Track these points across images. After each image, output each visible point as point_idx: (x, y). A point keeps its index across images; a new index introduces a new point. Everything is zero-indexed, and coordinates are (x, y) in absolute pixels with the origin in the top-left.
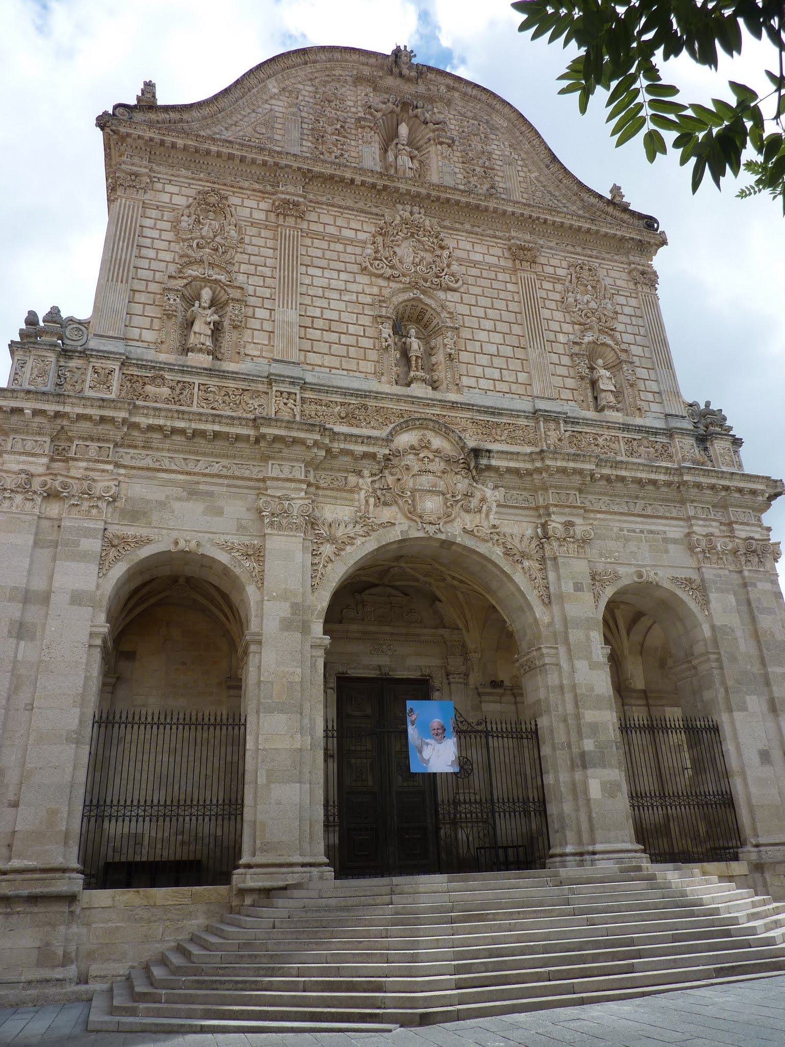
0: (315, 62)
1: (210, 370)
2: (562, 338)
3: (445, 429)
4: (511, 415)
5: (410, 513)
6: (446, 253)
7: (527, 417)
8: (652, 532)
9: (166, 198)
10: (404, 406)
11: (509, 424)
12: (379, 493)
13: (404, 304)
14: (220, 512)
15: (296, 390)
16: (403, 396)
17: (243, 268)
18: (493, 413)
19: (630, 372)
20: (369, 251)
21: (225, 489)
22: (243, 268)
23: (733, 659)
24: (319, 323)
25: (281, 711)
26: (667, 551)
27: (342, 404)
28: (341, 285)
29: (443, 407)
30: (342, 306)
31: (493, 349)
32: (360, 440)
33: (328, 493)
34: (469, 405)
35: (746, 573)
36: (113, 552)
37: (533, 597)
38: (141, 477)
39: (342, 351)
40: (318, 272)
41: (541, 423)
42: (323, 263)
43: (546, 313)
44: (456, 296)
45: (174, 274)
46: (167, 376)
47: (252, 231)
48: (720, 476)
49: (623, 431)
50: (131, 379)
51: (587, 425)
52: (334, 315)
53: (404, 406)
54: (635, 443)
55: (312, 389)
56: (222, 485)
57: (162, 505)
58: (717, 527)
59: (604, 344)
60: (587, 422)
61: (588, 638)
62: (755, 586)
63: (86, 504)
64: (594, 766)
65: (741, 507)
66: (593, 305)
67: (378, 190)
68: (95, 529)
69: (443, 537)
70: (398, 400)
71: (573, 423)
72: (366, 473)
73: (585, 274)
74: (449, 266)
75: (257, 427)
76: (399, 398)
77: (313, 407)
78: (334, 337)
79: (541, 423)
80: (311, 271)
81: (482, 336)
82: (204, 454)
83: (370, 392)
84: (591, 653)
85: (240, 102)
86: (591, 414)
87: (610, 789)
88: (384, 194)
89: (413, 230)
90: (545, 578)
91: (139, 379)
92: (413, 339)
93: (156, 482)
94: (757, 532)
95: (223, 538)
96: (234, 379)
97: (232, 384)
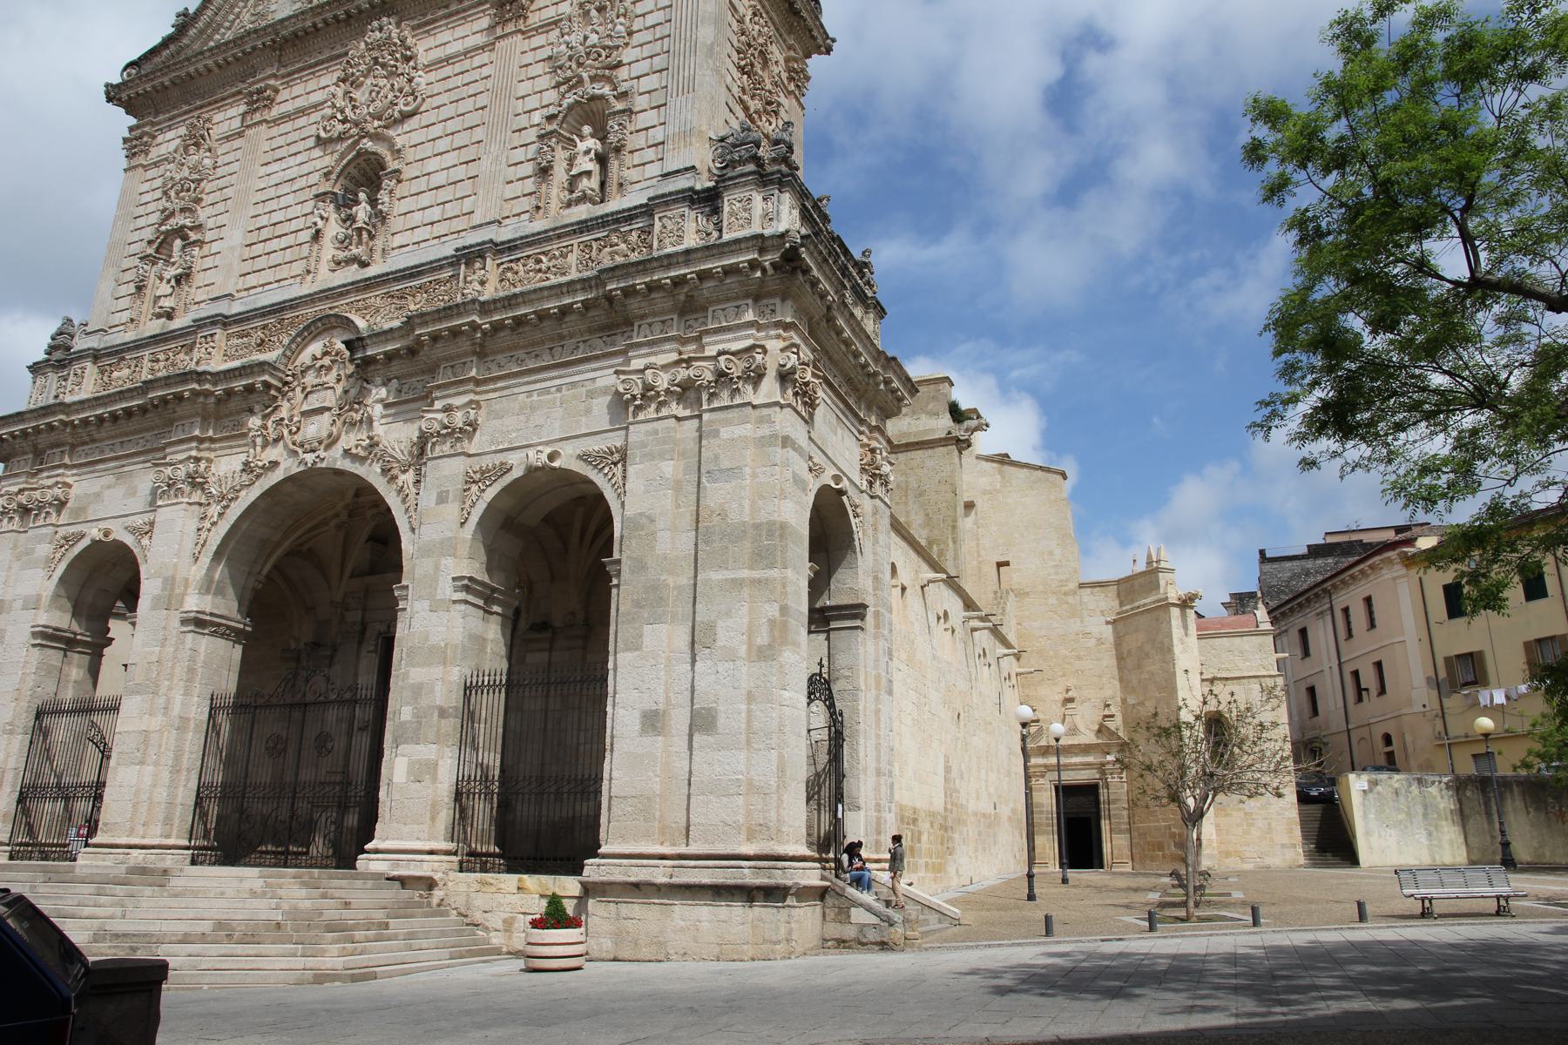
1: (154, 336)
4: (433, 270)
5: (294, 444)
7: (451, 264)
13: (353, 165)
16: (316, 293)
19: (616, 127)
21: (141, 466)
23: (640, 566)
24: (265, 234)
25: (138, 693)
26: (588, 411)
27: (264, 327)
29: (358, 290)
32: (237, 373)
34: (383, 275)
41: (463, 266)
44: (413, 122)
45: (151, 238)
48: (665, 263)
49: (582, 232)
51: (530, 244)
54: (595, 245)
55: (236, 322)
57: (98, 495)
58: (671, 351)
59: (593, 98)
61: (437, 568)
62: (716, 433)
64: (405, 742)
65: (728, 300)
67: (344, 21)
68: (46, 534)
70: (313, 301)
71: (509, 248)
72: (257, 408)
79: (463, 266)
82: (132, 433)
83: (284, 302)
87: (431, 769)
88: (352, 21)
91: (108, 368)
92: (364, 204)
94: (747, 337)
96: (174, 338)
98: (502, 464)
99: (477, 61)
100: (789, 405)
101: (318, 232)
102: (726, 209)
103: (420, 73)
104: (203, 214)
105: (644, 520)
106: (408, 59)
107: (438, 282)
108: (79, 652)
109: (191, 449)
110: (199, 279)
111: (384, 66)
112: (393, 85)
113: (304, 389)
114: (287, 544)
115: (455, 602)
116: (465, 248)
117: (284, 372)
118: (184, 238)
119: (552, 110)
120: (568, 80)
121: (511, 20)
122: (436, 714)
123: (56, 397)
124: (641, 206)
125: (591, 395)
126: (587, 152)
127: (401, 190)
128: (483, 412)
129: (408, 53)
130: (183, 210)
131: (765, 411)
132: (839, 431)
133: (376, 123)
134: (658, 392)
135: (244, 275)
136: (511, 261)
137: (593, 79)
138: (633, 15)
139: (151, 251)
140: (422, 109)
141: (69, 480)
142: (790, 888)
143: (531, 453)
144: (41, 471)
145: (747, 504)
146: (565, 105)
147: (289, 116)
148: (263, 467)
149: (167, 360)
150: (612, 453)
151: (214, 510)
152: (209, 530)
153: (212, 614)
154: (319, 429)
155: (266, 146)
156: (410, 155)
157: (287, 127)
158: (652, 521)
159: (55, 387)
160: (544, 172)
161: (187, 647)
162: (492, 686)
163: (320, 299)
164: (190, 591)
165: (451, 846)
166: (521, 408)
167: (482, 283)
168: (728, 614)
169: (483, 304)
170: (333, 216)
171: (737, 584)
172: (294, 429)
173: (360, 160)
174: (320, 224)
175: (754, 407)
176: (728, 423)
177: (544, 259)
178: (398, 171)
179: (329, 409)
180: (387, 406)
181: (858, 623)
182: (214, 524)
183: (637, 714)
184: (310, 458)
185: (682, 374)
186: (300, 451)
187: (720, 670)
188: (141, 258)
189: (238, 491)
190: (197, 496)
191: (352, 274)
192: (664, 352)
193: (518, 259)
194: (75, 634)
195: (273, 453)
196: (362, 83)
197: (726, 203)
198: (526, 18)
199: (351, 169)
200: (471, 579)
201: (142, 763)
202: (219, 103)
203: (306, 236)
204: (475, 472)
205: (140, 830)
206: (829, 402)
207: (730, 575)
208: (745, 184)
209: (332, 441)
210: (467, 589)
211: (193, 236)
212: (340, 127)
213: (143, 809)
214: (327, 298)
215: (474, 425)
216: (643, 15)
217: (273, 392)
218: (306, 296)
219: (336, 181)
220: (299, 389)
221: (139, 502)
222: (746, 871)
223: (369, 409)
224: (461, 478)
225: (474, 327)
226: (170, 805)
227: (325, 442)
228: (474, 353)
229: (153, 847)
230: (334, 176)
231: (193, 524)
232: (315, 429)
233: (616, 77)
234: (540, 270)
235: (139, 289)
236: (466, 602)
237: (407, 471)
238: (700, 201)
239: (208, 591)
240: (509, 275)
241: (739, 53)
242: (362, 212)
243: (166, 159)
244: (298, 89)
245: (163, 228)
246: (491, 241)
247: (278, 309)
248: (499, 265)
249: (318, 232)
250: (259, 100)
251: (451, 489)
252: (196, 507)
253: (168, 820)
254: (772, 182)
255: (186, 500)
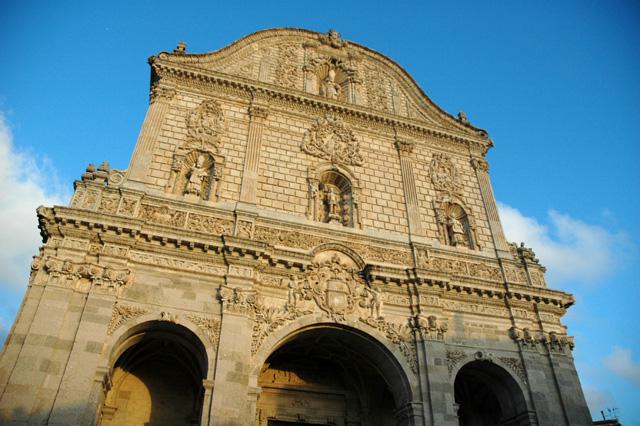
2: (429, 199)
3: (349, 253)
6: (356, 143)
7: (405, 247)
8: (488, 326)
9: (183, 104)
10: (323, 235)
12: (303, 291)
14: (193, 297)
15: (252, 220)
17: (226, 145)
20: (307, 139)
21: (198, 281)
22: (226, 145)
24: (271, 181)
27: (283, 232)
28: (287, 159)
30: (287, 171)
31: (384, 203)
33: (269, 289)
35: (552, 357)
36: (120, 318)
37: (407, 368)
38: (145, 270)
39: (285, 198)
40: (273, 150)
42: (277, 145)
43: (418, 183)
44: (360, 169)
46: (170, 207)
47: (233, 124)
50: (147, 207)
52: (282, 177)
53: (323, 235)
56: (197, 279)
60: (444, 252)
62: (558, 365)
63: (106, 284)
66: (448, 179)
69: (345, 323)
73: (443, 161)
74: (357, 151)
75: (223, 242)
76: (321, 230)
77: (263, 232)
78: (280, 189)
80: (268, 149)
81: (378, 194)
86: (448, 247)
89: (336, 129)
90: (417, 355)
95: (194, 314)
96: (213, 212)
97: (211, 215)
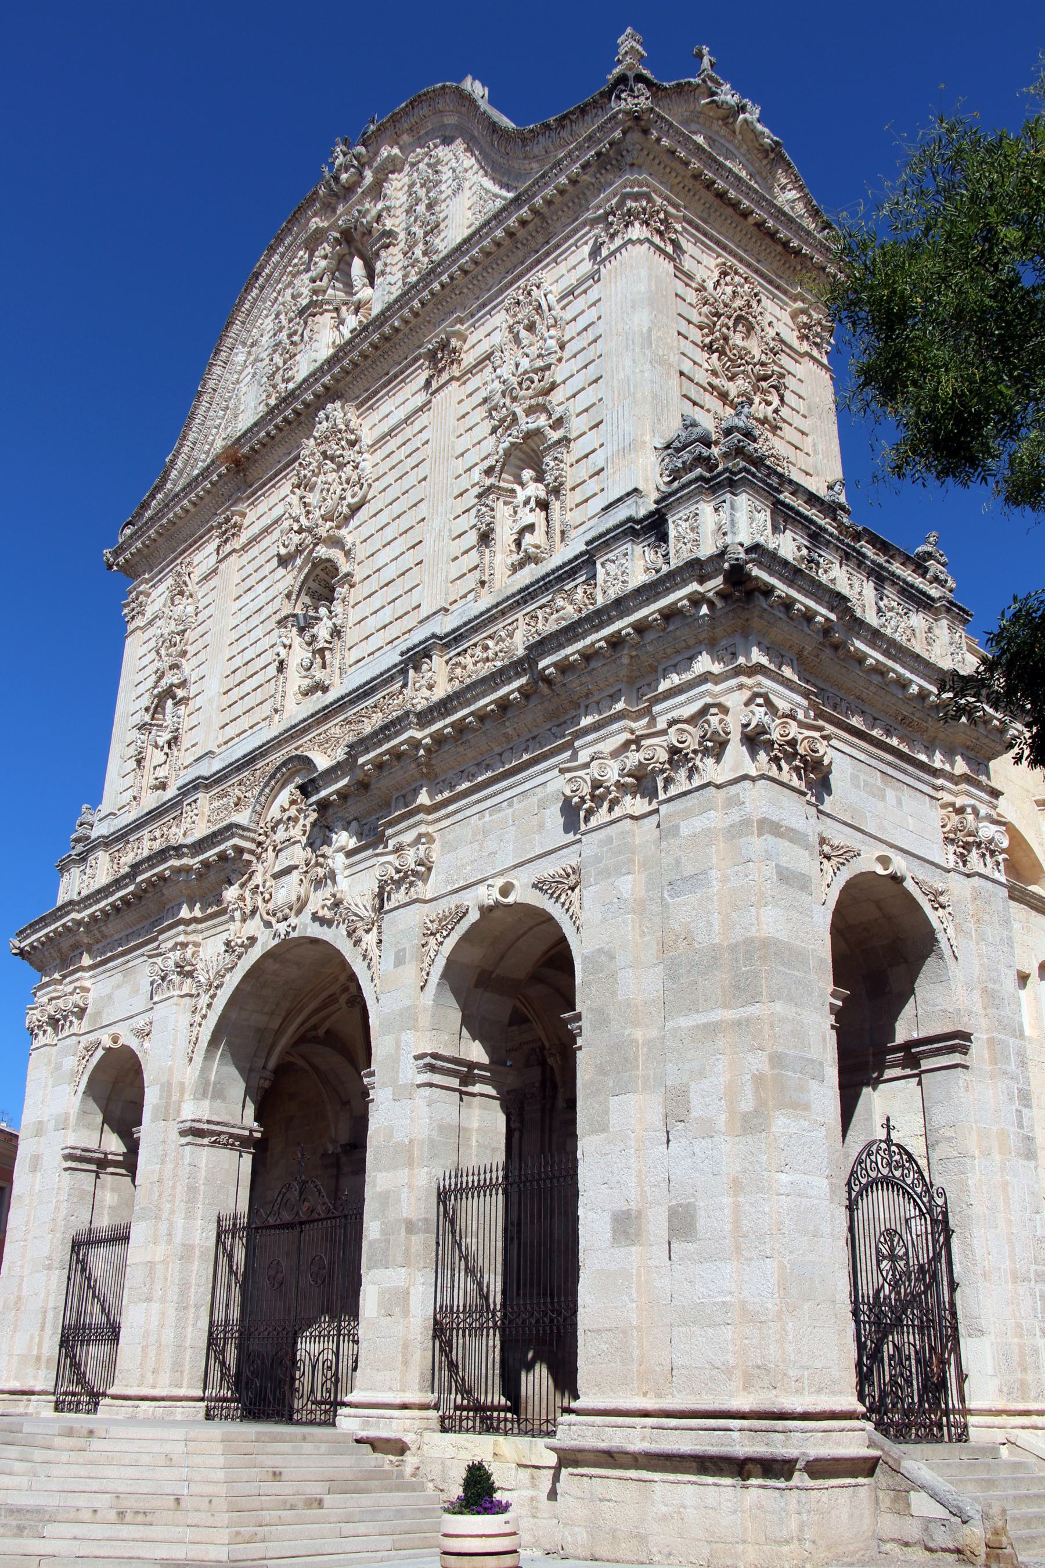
0: (269, 276)
5: (268, 914)
11: (384, 697)
16: (281, 734)
18: (366, 694)
19: (552, 464)
23: (603, 1020)
24: (239, 676)
26: (541, 826)
49: (526, 602)
51: (475, 630)
57: (110, 997)
59: (529, 435)
61: (398, 1046)
62: (675, 831)
71: (455, 639)
84: (397, 1072)
85: (211, 413)
93: (108, 974)
96: (167, 811)
98: (457, 907)
99: (417, 426)
100: (762, 777)
101: (281, 662)
102: (672, 533)
103: (366, 456)
104: (187, 666)
105: (603, 957)
106: (352, 444)
107: (391, 695)
108: (112, 1174)
109: (178, 934)
110: (186, 741)
111: (332, 459)
112: (340, 477)
113: (275, 847)
114: (291, 1030)
115: (419, 1086)
116: (409, 650)
117: (255, 832)
118: (174, 697)
119: (491, 461)
120: (502, 421)
121: (444, 368)
122: (403, 1230)
123: (79, 893)
124: (582, 554)
125: (543, 805)
126: (527, 502)
127: (354, 595)
128: (436, 847)
129: (353, 437)
130: (171, 668)
131: (734, 789)
132: (890, 794)
133: (329, 524)
134: (607, 788)
135: (223, 727)
136: (459, 654)
137: (530, 411)
138: (563, 323)
139: (147, 718)
140: (369, 497)
141: (87, 984)
142: (796, 1460)
143: (482, 889)
144: (64, 977)
145: (716, 919)
146: (501, 452)
147: (255, 539)
148: (242, 946)
149: (162, 836)
150: (568, 875)
151: (204, 1000)
152: (200, 1025)
153: (209, 1122)
154: (288, 893)
155: (237, 578)
156: (361, 553)
157: (254, 551)
158: (612, 958)
159: (77, 883)
160: (485, 538)
161: (186, 1162)
162: (483, 1188)
163: (286, 740)
164: (186, 1097)
165: (431, 1398)
166: (474, 834)
167: (430, 687)
168: (702, 1074)
169: (419, 715)
170: (297, 641)
171: (711, 1030)
172: (267, 896)
173: (318, 571)
174: (283, 652)
175: (718, 787)
176: (688, 814)
177: (490, 643)
178: (348, 575)
179: (296, 867)
180: (350, 854)
181: (956, 1058)
182: (204, 1017)
183: (607, 1217)
184: (282, 928)
185: (633, 758)
186: (273, 920)
187: (697, 1150)
188: (139, 729)
189: (223, 977)
190: (188, 986)
191: (320, 701)
192: (611, 735)
193: (465, 651)
194: (106, 1154)
195: (254, 926)
196: (316, 483)
197: (671, 526)
198: (459, 362)
199: (311, 583)
200: (435, 1056)
201: (149, 1300)
202: (195, 542)
203: (272, 670)
204: (431, 922)
205: (150, 1378)
206: (862, 757)
207: (701, 1019)
208: (689, 497)
209: (302, 904)
210: (432, 1068)
211: (180, 693)
212: (296, 539)
213: (152, 1352)
214: (292, 737)
215: (426, 866)
216: (574, 319)
217: (246, 856)
218: (272, 740)
219: (296, 600)
220: (271, 848)
221: (141, 1002)
222: (736, 1435)
223: (330, 861)
224: (418, 931)
225: (415, 744)
226: (179, 1347)
227: (295, 908)
228: (423, 775)
229: (163, 1399)
230: (294, 597)
231: (185, 1018)
232: (287, 891)
233: (550, 402)
234: (487, 659)
235: (139, 762)
236: (431, 1085)
237: (370, 930)
238: (646, 530)
239: (204, 1095)
240: (458, 671)
241: (701, 328)
242: (322, 631)
243: (157, 617)
244: (263, 507)
245: (156, 692)
246: (434, 636)
247: (249, 760)
248: (447, 662)
249: (281, 662)
250: (230, 530)
251: (407, 946)
252: (187, 999)
253: (177, 1367)
254: (720, 486)
255: (177, 993)
